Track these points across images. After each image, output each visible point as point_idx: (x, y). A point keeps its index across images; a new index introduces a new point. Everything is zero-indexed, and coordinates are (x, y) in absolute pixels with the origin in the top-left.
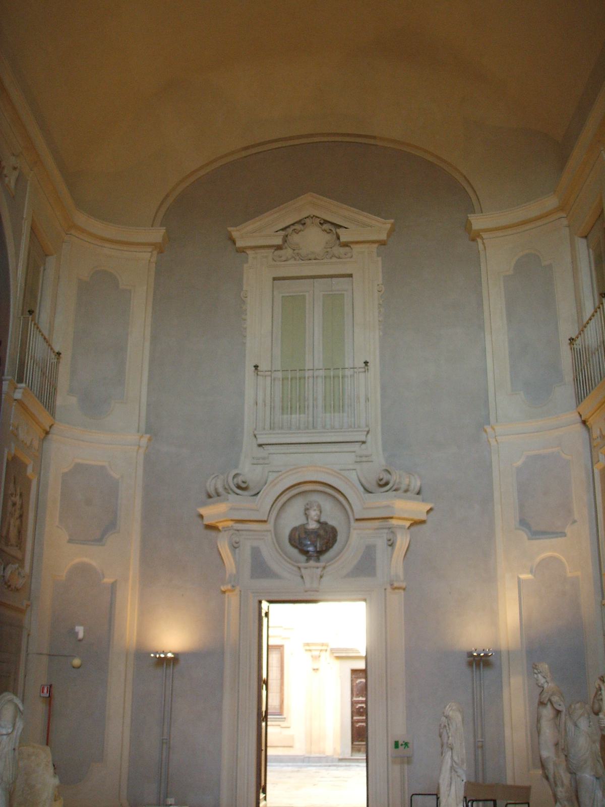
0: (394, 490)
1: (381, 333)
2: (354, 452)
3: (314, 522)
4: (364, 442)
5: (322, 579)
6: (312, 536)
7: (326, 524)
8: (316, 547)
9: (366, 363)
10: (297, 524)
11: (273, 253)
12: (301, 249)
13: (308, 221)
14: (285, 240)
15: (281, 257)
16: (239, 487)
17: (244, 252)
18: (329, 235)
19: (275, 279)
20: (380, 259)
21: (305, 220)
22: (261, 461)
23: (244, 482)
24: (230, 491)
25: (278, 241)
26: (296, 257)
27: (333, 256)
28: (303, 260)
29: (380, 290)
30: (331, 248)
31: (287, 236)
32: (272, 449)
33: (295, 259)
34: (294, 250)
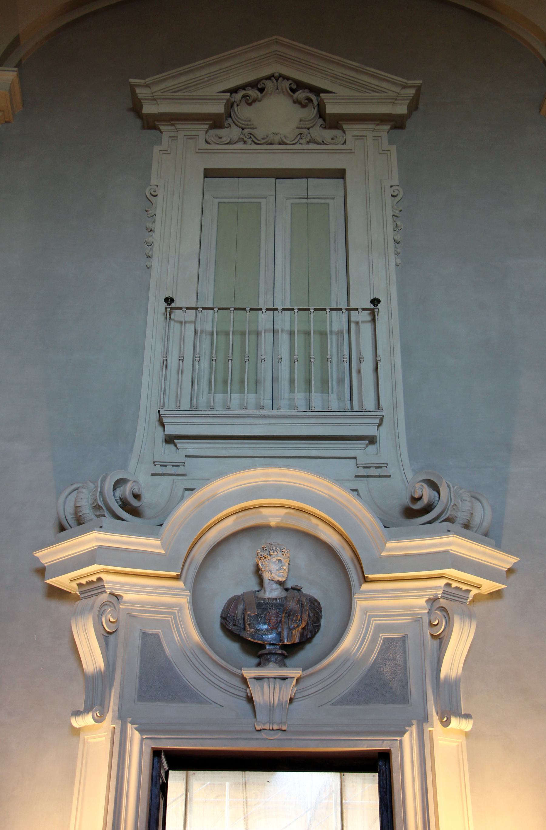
0: (444, 521)
1: (398, 261)
2: (355, 458)
3: (275, 586)
4: (372, 440)
5: (291, 706)
6: (273, 612)
7: (297, 589)
8: (280, 634)
9: (375, 302)
10: (239, 591)
11: (207, 132)
12: (256, 128)
13: (269, 85)
14: (230, 105)
15: (221, 138)
16: (125, 505)
17: (156, 128)
18: (305, 110)
19: (209, 173)
20: (393, 148)
21: (264, 81)
22: (170, 470)
23: (137, 496)
24: (106, 513)
25: (218, 108)
26: (245, 139)
27: (313, 141)
28: (257, 144)
29: (394, 194)
30: (308, 129)
31: (232, 106)
32: (191, 447)
33: (245, 142)
34: (243, 129)
